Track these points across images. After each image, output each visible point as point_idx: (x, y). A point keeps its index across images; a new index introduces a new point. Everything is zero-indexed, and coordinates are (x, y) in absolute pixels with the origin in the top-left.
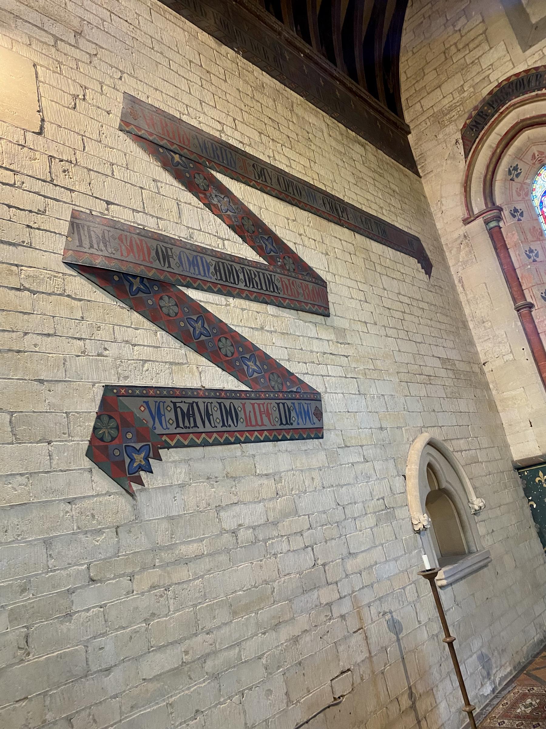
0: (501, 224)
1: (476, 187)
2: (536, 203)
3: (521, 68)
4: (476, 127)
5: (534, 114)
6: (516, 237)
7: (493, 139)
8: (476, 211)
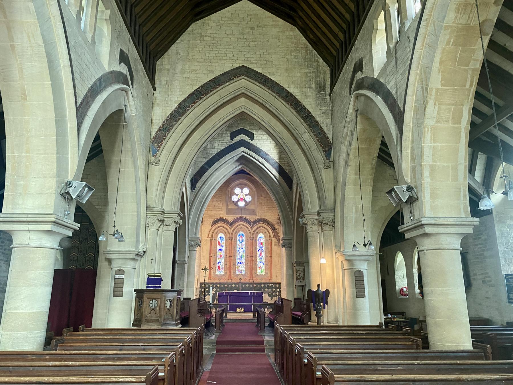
1: (211, 232)
4: (215, 222)
7: (216, 226)
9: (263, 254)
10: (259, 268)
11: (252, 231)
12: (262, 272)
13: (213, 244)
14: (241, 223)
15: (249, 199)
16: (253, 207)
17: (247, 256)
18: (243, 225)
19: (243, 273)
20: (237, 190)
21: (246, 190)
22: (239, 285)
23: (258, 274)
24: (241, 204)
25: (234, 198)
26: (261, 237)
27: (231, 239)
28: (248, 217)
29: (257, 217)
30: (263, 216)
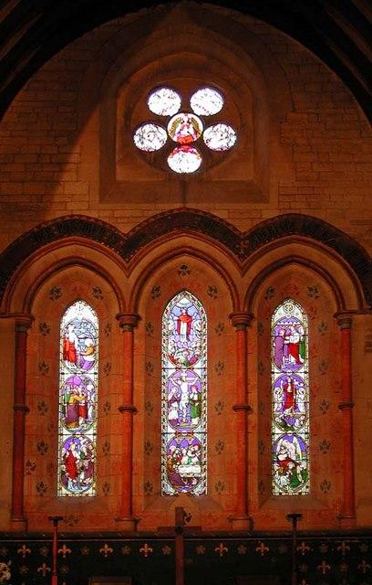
0: (29, 331)
2: (62, 326)
3: (94, 215)
5: (88, 257)
6: (36, 349)
8: (12, 311)
9: (301, 398)
10: (283, 464)
11: (243, 282)
12: (293, 480)
13: (32, 346)
14: (187, 240)
15: (221, 138)
16: (245, 173)
17: (217, 408)
18: (194, 253)
19: (198, 490)
20: (163, 101)
21: (208, 101)
22: (172, 544)
23: (277, 491)
24: (184, 163)
25: (149, 139)
26: (290, 318)
27: (133, 330)
28: (221, 212)
29: (270, 212)
30: (300, 207)
